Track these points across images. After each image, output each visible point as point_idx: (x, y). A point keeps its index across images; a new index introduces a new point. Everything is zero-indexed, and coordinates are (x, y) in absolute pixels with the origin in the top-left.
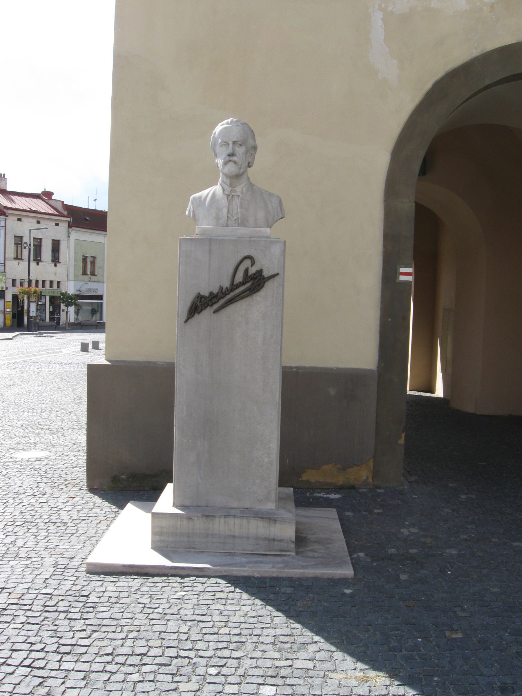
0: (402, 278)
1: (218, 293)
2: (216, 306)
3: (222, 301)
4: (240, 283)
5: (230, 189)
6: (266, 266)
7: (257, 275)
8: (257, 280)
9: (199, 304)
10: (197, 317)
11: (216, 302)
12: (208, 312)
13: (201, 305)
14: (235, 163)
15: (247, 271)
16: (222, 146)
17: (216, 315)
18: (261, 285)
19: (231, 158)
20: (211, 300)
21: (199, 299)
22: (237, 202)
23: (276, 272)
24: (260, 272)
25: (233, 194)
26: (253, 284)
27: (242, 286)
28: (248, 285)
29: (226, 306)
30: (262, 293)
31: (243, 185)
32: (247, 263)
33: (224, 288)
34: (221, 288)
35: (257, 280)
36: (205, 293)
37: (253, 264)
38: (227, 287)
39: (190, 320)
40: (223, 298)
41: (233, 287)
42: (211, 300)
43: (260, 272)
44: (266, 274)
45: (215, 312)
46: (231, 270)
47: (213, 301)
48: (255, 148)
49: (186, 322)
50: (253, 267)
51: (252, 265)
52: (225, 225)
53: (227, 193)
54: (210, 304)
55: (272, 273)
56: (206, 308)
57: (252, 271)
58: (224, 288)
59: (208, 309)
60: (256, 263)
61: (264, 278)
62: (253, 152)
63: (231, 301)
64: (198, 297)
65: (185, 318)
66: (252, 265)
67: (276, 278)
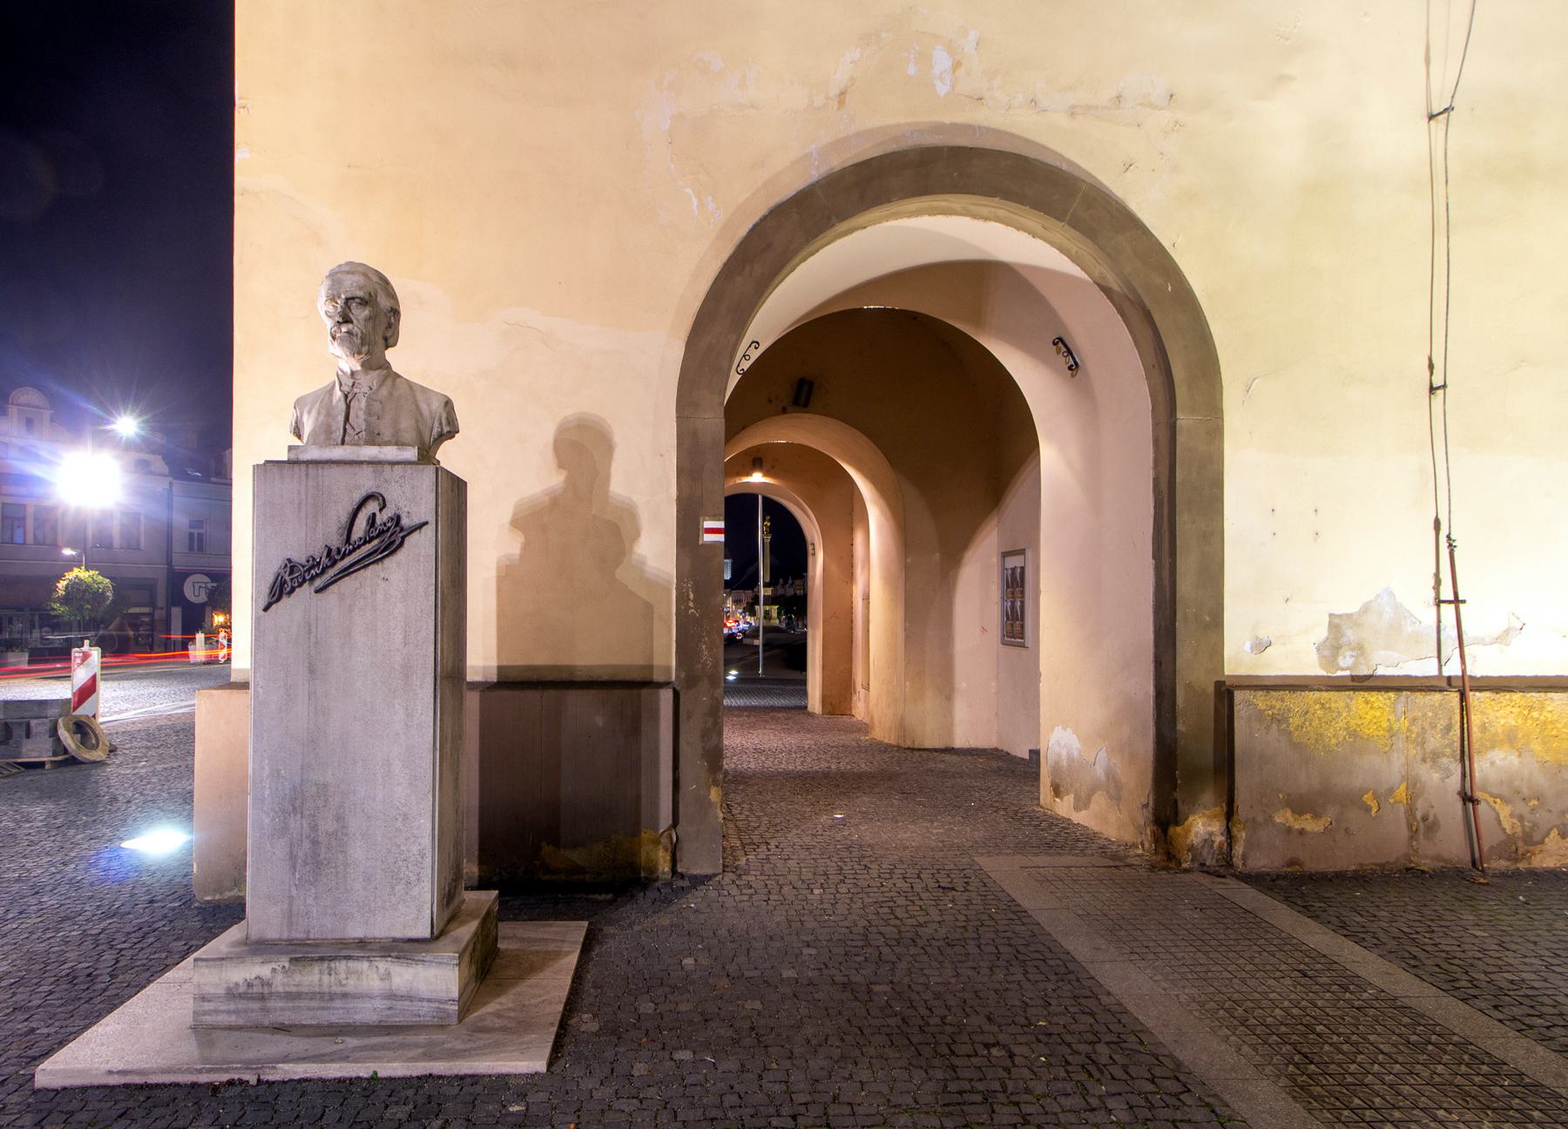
0: (708, 538)
2: (319, 583)
3: (331, 572)
12: (306, 591)
17: (319, 595)
28: (376, 542)
30: (401, 555)
32: (372, 507)
33: (334, 548)
36: (300, 557)
37: (383, 507)
44: (405, 522)
45: (318, 591)
46: (345, 518)
49: (266, 609)
55: (417, 521)
56: (300, 585)
57: (381, 518)
58: (334, 548)
63: (346, 572)
65: (263, 604)
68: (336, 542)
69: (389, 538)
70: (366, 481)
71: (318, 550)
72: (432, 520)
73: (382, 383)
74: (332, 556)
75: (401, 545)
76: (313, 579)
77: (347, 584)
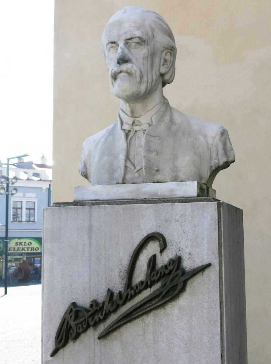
1: (104, 303)
2: (102, 327)
3: (113, 318)
4: (142, 283)
5: (129, 120)
6: (188, 251)
7: (170, 268)
8: (171, 277)
9: (72, 323)
10: (72, 348)
11: (101, 321)
12: (90, 337)
13: (77, 325)
14: (129, 74)
15: (153, 260)
16: (109, 50)
17: (103, 342)
18: (179, 288)
19: (125, 67)
20: (93, 315)
21: (73, 314)
22: (140, 141)
23: (205, 262)
24: (177, 261)
25: (136, 128)
26: (164, 286)
27: (145, 288)
28: (157, 286)
29: (119, 327)
30: (184, 300)
31: (153, 112)
32: (153, 248)
33: (116, 292)
34: (110, 293)
35: (171, 277)
36: (85, 301)
37: (164, 247)
38: (120, 292)
39: (61, 351)
40: (115, 311)
41: (131, 289)
42: (93, 315)
43: (177, 261)
44: (188, 264)
45: (103, 336)
46: (126, 261)
47: (96, 318)
48: (172, 50)
49: (54, 354)
50: (165, 253)
51: (161, 252)
52: (120, 181)
53: (126, 127)
54: (91, 323)
55: (199, 263)
56: (85, 330)
57: (163, 260)
58: (116, 292)
59: (91, 331)
60: (169, 246)
61: (184, 272)
62: (168, 57)
63: (129, 318)
64: (71, 310)
65: (51, 346)
66: (161, 252)
67: (207, 272)
68: (118, 285)
69: (169, 281)
70: (148, 221)
71: (101, 296)
72: (215, 262)
73: (161, 119)
74: (114, 300)
75: (183, 289)
76: (96, 325)
77: (130, 331)
